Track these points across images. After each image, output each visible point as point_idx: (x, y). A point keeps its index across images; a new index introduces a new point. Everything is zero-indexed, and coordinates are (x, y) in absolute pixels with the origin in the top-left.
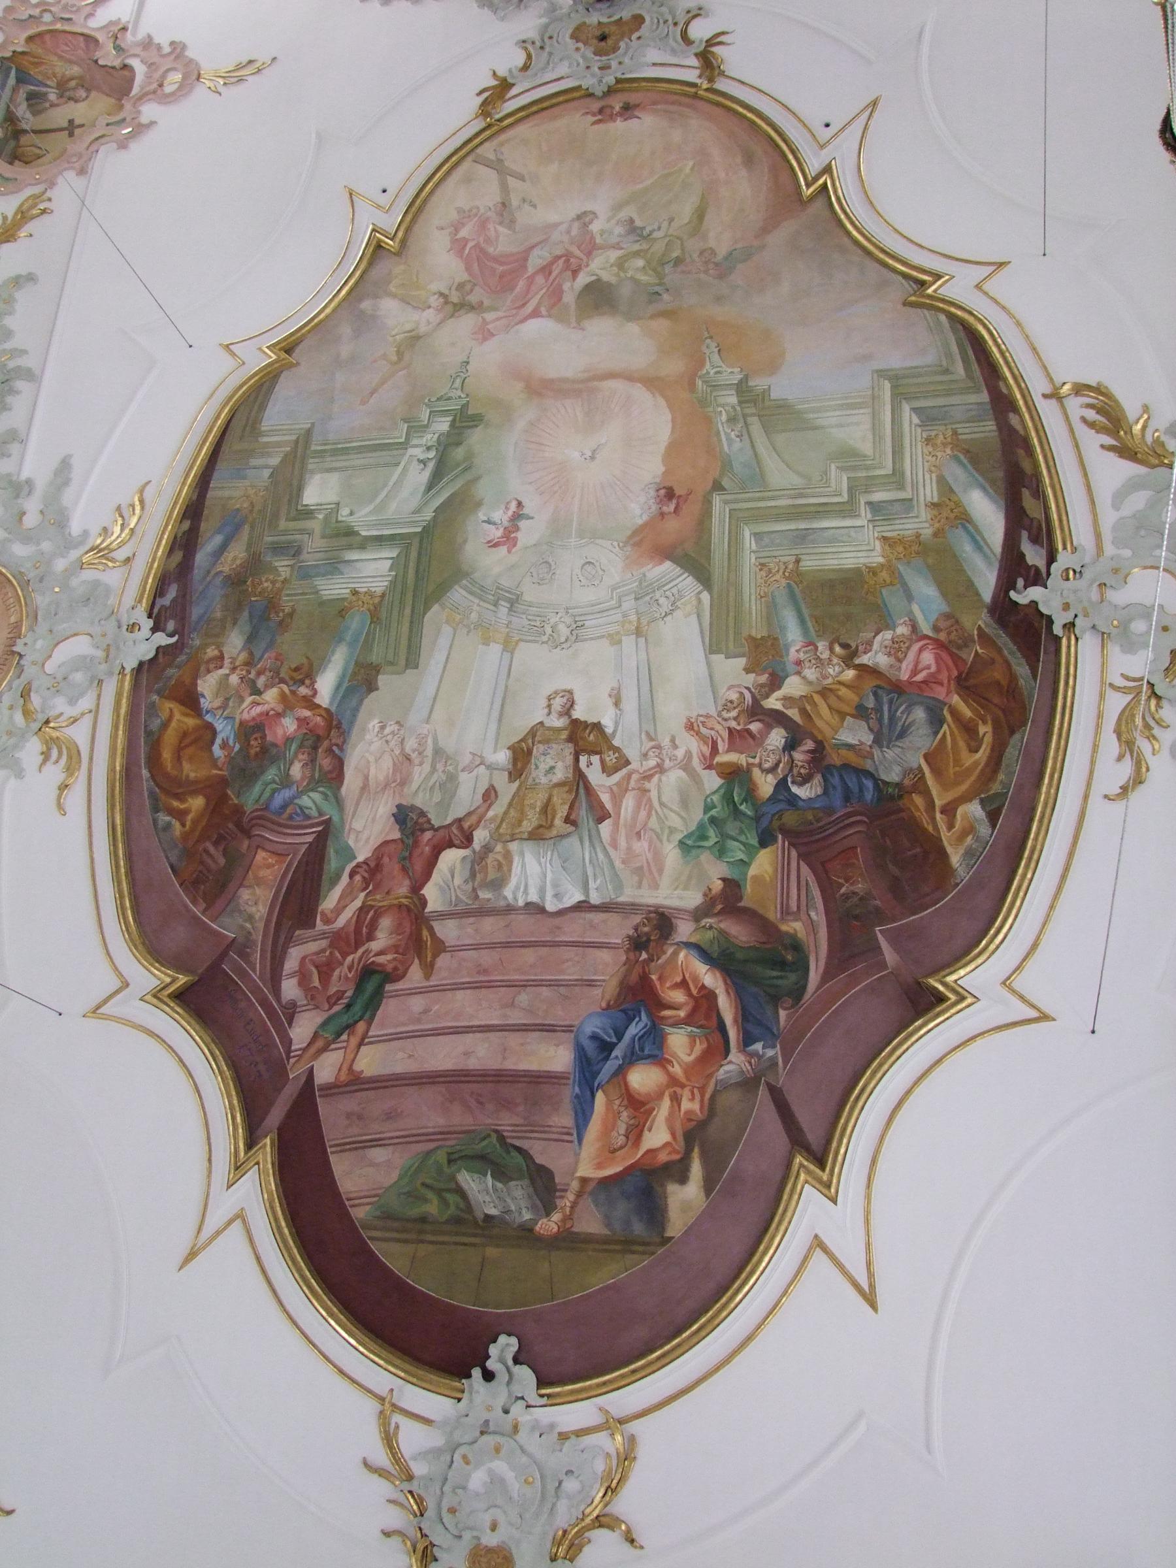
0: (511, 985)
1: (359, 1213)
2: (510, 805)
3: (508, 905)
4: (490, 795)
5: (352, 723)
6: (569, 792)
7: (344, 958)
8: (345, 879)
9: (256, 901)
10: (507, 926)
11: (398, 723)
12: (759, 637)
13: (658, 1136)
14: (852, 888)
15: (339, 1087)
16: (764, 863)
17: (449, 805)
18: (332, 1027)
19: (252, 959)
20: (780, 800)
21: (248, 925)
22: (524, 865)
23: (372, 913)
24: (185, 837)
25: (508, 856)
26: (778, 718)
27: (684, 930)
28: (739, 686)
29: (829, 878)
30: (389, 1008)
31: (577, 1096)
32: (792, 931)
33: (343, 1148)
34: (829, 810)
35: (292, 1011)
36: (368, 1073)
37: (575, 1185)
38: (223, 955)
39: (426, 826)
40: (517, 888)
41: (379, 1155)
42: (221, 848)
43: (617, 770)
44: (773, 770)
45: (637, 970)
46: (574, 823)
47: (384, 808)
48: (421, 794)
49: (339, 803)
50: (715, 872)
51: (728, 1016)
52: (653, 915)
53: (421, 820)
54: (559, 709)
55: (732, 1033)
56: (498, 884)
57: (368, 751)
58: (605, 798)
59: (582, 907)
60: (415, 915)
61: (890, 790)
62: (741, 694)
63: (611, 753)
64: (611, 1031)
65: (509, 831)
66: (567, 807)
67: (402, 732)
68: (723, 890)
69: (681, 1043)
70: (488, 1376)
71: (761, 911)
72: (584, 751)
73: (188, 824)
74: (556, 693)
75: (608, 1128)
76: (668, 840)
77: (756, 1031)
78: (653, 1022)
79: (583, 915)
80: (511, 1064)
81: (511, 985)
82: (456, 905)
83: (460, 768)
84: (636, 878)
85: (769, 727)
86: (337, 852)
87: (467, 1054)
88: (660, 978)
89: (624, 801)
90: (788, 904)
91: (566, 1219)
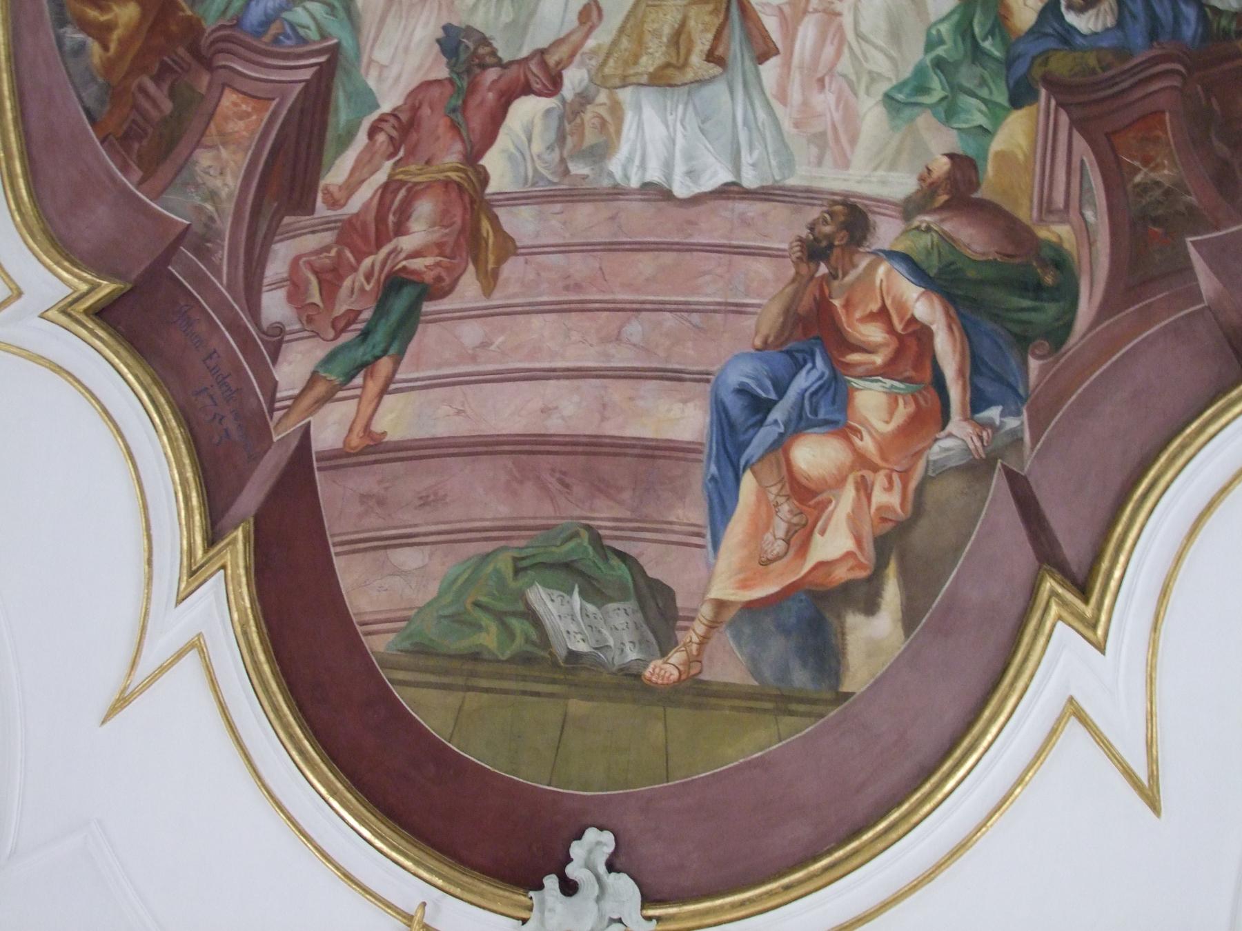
0: (615, 308)
1: (378, 644)
2: (622, 30)
3: (616, 186)
6: (715, 12)
7: (359, 261)
8: (362, 138)
9: (221, 170)
10: (612, 218)
13: (834, 543)
14: (1152, 175)
15: (349, 455)
16: (1016, 133)
17: (526, 27)
18: (341, 365)
19: (215, 259)
20: (1046, 35)
21: (209, 207)
22: (640, 126)
23: (402, 193)
24: (109, 66)
25: (616, 109)
27: (887, 232)
29: (1116, 157)
30: (427, 338)
31: (713, 479)
32: (1054, 239)
33: (357, 546)
34: (1122, 53)
35: (277, 339)
36: (394, 435)
37: (706, 611)
38: (171, 251)
39: (489, 60)
40: (630, 160)
41: (408, 558)
42: (166, 87)
45: (813, 289)
47: (424, 31)
50: (938, 145)
51: (950, 368)
52: (838, 208)
53: (481, 51)
55: (955, 392)
56: (599, 154)
58: (771, 24)
59: (729, 192)
60: (470, 198)
61: (1224, 22)
64: (768, 383)
65: (619, 72)
66: (710, 36)
68: (950, 177)
69: (874, 405)
70: (569, 888)
71: (1007, 207)
73: (113, 46)
75: (759, 528)
76: (868, 93)
77: (990, 389)
78: (833, 370)
79: (730, 204)
80: (611, 429)
81: (615, 308)
82: (533, 185)
84: (814, 151)
86: (349, 98)
87: (546, 411)
88: (848, 305)
89: (801, 30)
90: (1050, 201)
91: (689, 662)
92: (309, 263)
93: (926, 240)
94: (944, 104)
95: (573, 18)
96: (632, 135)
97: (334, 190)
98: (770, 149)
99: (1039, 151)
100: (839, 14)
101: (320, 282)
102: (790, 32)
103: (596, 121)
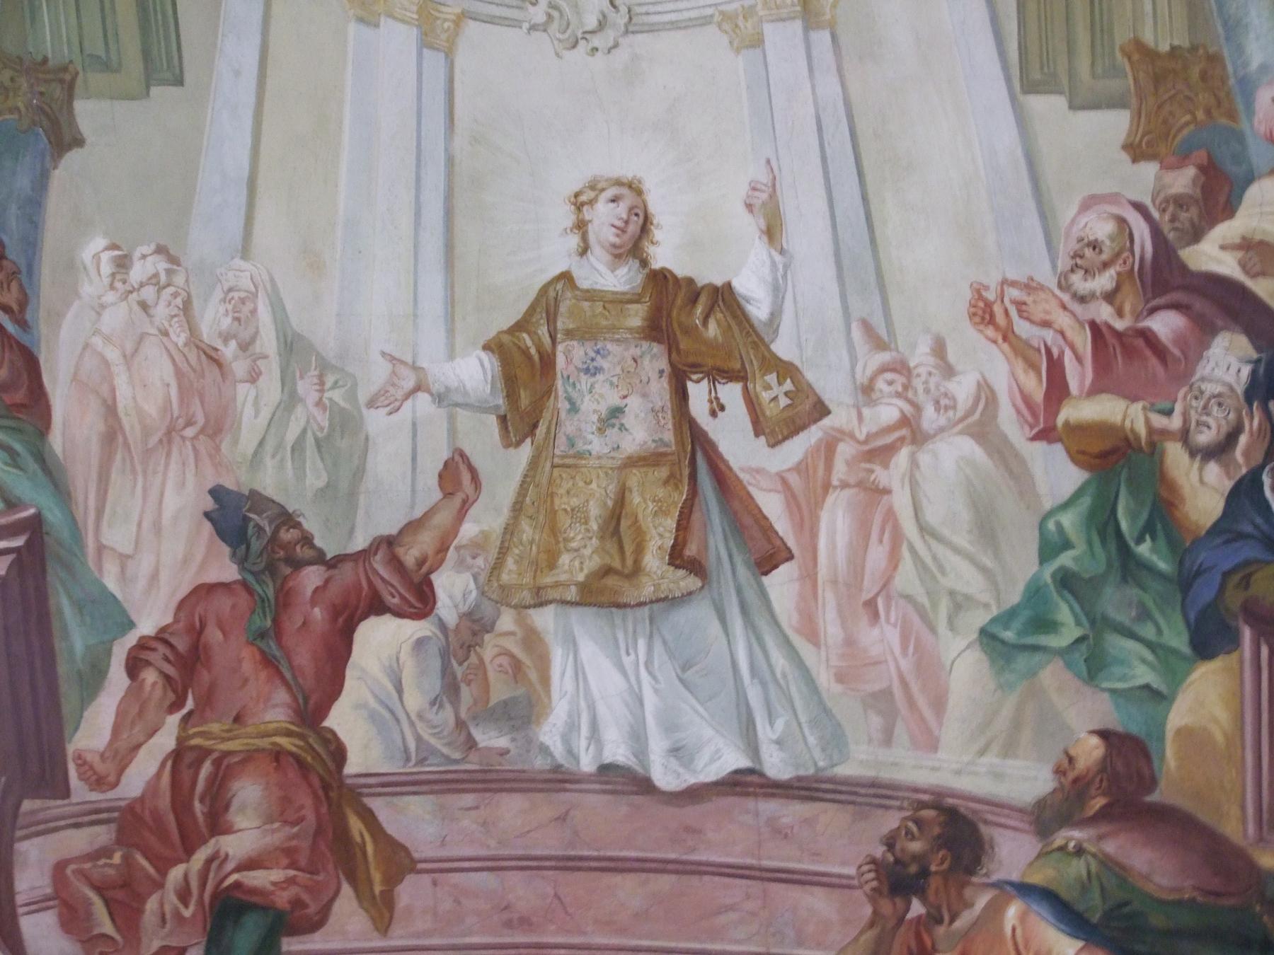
2: (518, 508)
3: (557, 768)
4: (458, 476)
5: (32, 244)
7: (163, 873)
10: (562, 819)
11: (160, 250)
12: (1164, 47)
16: (1206, 699)
17: (352, 495)
20: (1241, 536)
23: (206, 769)
25: (532, 640)
26: (1225, 303)
27: (1013, 854)
28: (1113, 198)
39: (301, 552)
40: (572, 726)
43: (793, 427)
44: (1221, 450)
46: (696, 567)
47: (180, 496)
48: (269, 463)
49: (52, 473)
50: (1083, 719)
52: (928, 814)
53: (287, 535)
54: (610, 236)
56: (522, 713)
57: (97, 332)
58: (772, 506)
59: (744, 783)
62: (1121, 221)
63: (772, 378)
66: (671, 523)
67: (179, 280)
68: (1105, 765)
71: (1204, 817)
72: (695, 367)
74: (594, 186)
79: (750, 803)
82: (421, 762)
83: (363, 397)
84: (876, 721)
85: (1205, 329)
86: (79, 606)
92: (81, 873)
93: (1078, 868)
94: (1083, 647)
95: (430, 492)
96: (569, 685)
97: (95, 760)
98: (803, 719)
99: (1249, 729)
100: (887, 491)
101: (108, 903)
102: (807, 521)
103: (504, 660)
